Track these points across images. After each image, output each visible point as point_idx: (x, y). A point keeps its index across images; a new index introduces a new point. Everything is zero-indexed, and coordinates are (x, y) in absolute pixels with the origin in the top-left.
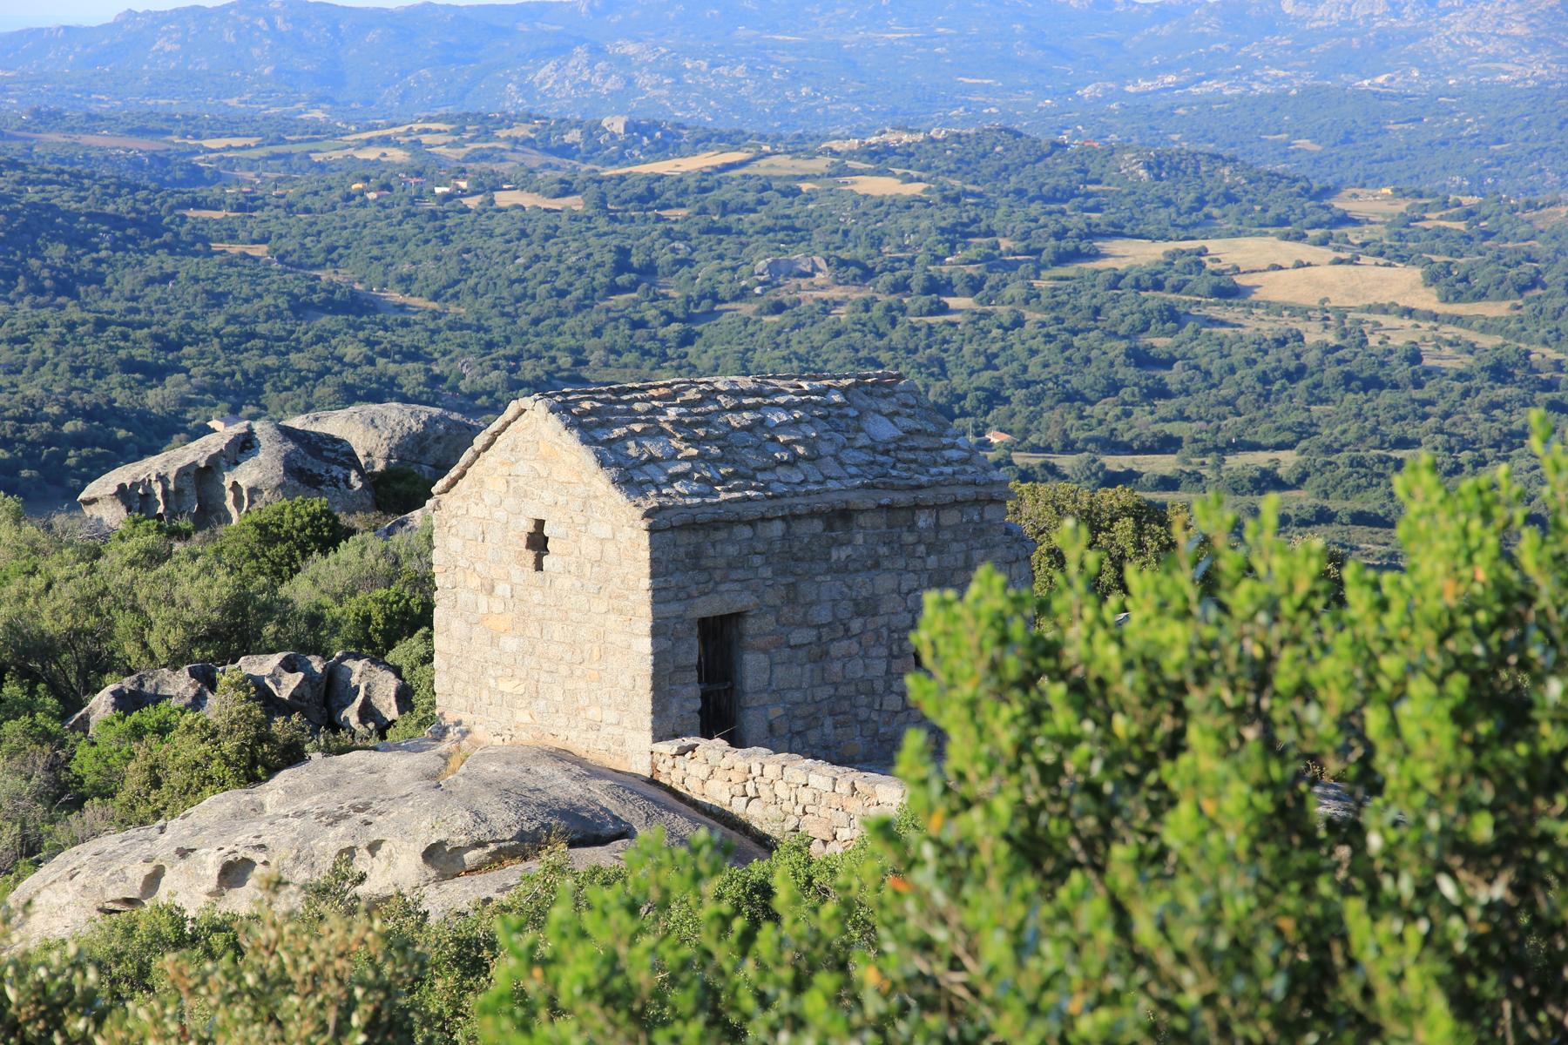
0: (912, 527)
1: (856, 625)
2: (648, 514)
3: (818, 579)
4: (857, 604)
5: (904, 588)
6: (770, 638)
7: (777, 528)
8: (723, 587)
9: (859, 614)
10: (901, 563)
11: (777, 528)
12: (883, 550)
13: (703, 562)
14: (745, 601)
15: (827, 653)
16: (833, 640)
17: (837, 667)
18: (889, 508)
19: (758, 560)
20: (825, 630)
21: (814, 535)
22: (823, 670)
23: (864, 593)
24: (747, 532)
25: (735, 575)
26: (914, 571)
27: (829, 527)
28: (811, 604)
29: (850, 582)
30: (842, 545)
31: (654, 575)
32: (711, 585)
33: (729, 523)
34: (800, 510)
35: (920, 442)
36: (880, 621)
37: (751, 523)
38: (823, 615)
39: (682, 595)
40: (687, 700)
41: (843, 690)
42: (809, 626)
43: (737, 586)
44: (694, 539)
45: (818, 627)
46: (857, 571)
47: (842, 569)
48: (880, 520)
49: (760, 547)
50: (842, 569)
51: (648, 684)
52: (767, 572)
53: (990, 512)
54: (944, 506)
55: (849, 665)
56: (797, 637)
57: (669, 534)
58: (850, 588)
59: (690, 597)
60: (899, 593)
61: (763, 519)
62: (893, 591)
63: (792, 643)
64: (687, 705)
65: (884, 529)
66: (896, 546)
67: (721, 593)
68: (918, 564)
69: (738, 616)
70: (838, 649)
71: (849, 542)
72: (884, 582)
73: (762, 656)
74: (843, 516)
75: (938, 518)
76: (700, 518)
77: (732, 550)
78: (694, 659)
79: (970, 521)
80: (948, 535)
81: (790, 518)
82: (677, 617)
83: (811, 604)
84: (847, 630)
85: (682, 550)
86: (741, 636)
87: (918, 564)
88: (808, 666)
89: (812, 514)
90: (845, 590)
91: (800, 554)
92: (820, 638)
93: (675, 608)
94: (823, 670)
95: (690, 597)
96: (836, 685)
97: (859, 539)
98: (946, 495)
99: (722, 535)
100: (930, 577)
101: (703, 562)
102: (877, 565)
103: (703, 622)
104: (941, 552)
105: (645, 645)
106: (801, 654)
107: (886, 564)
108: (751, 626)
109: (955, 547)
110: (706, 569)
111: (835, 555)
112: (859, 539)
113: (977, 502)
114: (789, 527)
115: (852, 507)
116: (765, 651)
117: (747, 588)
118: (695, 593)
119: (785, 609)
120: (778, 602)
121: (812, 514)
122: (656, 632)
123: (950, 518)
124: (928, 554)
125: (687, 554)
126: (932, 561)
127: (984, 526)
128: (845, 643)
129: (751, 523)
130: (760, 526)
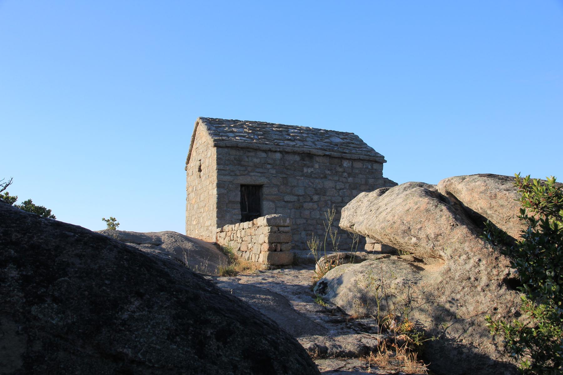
0: (341, 166)
1: (316, 198)
2: (215, 141)
3: (298, 178)
4: (316, 190)
5: (338, 187)
6: (275, 197)
7: (278, 156)
8: (252, 174)
9: (317, 194)
10: (336, 178)
11: (278, 156)
12: (328, 172)
13: (242, 163)
14: (261, 180)
15: (302, 207)
16: (305, 202)
17: (307, 212)
18: (330, 156)
19: (269, 166)
20: (301, 198)
21: (295, 161)
22: (301, 213)
23: (319, 186)
24: (264, 155)
25: (258, 170)
26: (342, 182)
27: (303, 159)
28: (294, 186)
29: (313, 181)
30: (308, 167)
31: (218, 164)
32: (246, 172)
33: (256, 150)
34: (288, 149)
35: (352, 145)
36: (327, 198)
37: (265, 151)
38: (301, 192)
39: (232, 174)
40: (235, 214)
41: (309, 222)
42: (293, 195)
43: (259, 175)
44: (238, 153)
45: (298, 196)
46: (316, 178)
47: (309, 176)
48: (326, 161)
49: (270, 161)
50: (309, 176)
51: (215, 206)
52: (274, 171)
53: (376, 166)
54: (355, 160)
55: (313, 213)
56: (287, 198)
57: (226, 150)
58: (313, 183)
59: (236, 175)
60: (336, 189)
61: (270, 151)
62: (333, 188)
63: (285, 200)
64: (234, 216)
65: (328, 164)
66: (334, 172)
67: (251, 176)
68: (344, 180)
69: (260, 187)
70: (306, 205)
71: (312, 167)
72: (328, 184)
73: (271, 203)
74: (310, 156)
75: (352, 164)
76: (240, 145)
77: (256, 160)
78: (238, 199)
79: (367, 168)
80: (357, 171)
81: (284, 152)
82: (230, 182)
83: (294, 186)
84: (312, 199)
85: (233, 157)
86: (262, 194)
87: (344, 180)
88: (293, 210)
89: (294, 153)
90: (311, 184)
91: (289, 167)
92: (299, 200)
93: (228, 178)
94: (301, 213)
95: (236, 175)
96: (307, 219)
97: (317, 166)
98: (356, 157)
99: (252, 154)
100: (350, 186)
101: (242, 163)
102: (325, 177)
103: (242, 186)
104: (355, 177)
105: (214, 192)
106: (290, 205)
107: (330, 177)
108: (265, 190)
109: (360, 176)
110: (244, 166)
111: (305, 170)
112: (317, 166)
113: (369, 161)
114: (283, 156)
115: (312, 153)
116: (273, 201)
117: (264, 176)
118: (238, 174)
119: (282, 187)
120: (279, 183)
121: (294, 153)
122: (219, 186)
123: (358, 165)
124: (349, 177)
125: (235, 159)
126: (350, 180)
127: (374, 171)
128: (311, 204)
129: (265, 151)
130: (270, 153)
